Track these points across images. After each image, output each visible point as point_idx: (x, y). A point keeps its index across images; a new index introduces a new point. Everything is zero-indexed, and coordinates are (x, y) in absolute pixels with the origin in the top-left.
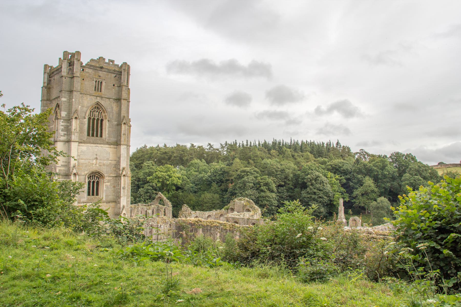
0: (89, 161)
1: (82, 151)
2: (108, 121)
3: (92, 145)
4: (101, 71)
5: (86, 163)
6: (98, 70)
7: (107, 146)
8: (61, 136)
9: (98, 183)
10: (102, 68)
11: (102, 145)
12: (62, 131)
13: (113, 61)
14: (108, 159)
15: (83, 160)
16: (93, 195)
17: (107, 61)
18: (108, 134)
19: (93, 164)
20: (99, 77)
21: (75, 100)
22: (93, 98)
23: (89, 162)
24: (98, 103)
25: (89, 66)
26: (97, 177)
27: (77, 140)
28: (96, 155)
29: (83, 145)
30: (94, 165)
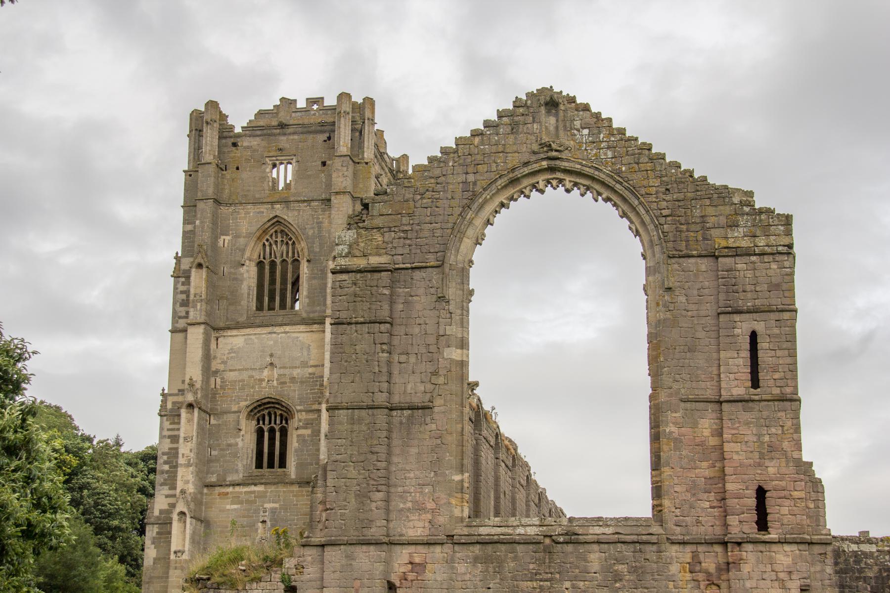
0: (250, 373)
1: (232, 351)
2: (308, 261)
3: (258, 330)
4: (285, 134)
5: (243, 381)
6: (275, 135)
7: (302, 328)
8: (180, 317)
9: (284, 432)
10: (282, 126)
11: (287, 328)
12: (182, 305)
13: (319, 101)
14: (304, 364)
15: (236, 373)
16: (271, 465)
17: (301, 104)
18: (308, 297)
19: (261, 380)
20: (279, 153)
21: (202, 222)
22: (263, 208)
23: (251, 377)
24: (277, 221)
25: (251, 129)
26: (281, 415)
27: (202, 320)
28: (271, 355)
29: (234, 332)
30: (264, 384)
